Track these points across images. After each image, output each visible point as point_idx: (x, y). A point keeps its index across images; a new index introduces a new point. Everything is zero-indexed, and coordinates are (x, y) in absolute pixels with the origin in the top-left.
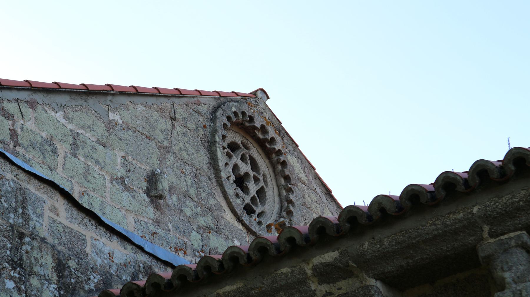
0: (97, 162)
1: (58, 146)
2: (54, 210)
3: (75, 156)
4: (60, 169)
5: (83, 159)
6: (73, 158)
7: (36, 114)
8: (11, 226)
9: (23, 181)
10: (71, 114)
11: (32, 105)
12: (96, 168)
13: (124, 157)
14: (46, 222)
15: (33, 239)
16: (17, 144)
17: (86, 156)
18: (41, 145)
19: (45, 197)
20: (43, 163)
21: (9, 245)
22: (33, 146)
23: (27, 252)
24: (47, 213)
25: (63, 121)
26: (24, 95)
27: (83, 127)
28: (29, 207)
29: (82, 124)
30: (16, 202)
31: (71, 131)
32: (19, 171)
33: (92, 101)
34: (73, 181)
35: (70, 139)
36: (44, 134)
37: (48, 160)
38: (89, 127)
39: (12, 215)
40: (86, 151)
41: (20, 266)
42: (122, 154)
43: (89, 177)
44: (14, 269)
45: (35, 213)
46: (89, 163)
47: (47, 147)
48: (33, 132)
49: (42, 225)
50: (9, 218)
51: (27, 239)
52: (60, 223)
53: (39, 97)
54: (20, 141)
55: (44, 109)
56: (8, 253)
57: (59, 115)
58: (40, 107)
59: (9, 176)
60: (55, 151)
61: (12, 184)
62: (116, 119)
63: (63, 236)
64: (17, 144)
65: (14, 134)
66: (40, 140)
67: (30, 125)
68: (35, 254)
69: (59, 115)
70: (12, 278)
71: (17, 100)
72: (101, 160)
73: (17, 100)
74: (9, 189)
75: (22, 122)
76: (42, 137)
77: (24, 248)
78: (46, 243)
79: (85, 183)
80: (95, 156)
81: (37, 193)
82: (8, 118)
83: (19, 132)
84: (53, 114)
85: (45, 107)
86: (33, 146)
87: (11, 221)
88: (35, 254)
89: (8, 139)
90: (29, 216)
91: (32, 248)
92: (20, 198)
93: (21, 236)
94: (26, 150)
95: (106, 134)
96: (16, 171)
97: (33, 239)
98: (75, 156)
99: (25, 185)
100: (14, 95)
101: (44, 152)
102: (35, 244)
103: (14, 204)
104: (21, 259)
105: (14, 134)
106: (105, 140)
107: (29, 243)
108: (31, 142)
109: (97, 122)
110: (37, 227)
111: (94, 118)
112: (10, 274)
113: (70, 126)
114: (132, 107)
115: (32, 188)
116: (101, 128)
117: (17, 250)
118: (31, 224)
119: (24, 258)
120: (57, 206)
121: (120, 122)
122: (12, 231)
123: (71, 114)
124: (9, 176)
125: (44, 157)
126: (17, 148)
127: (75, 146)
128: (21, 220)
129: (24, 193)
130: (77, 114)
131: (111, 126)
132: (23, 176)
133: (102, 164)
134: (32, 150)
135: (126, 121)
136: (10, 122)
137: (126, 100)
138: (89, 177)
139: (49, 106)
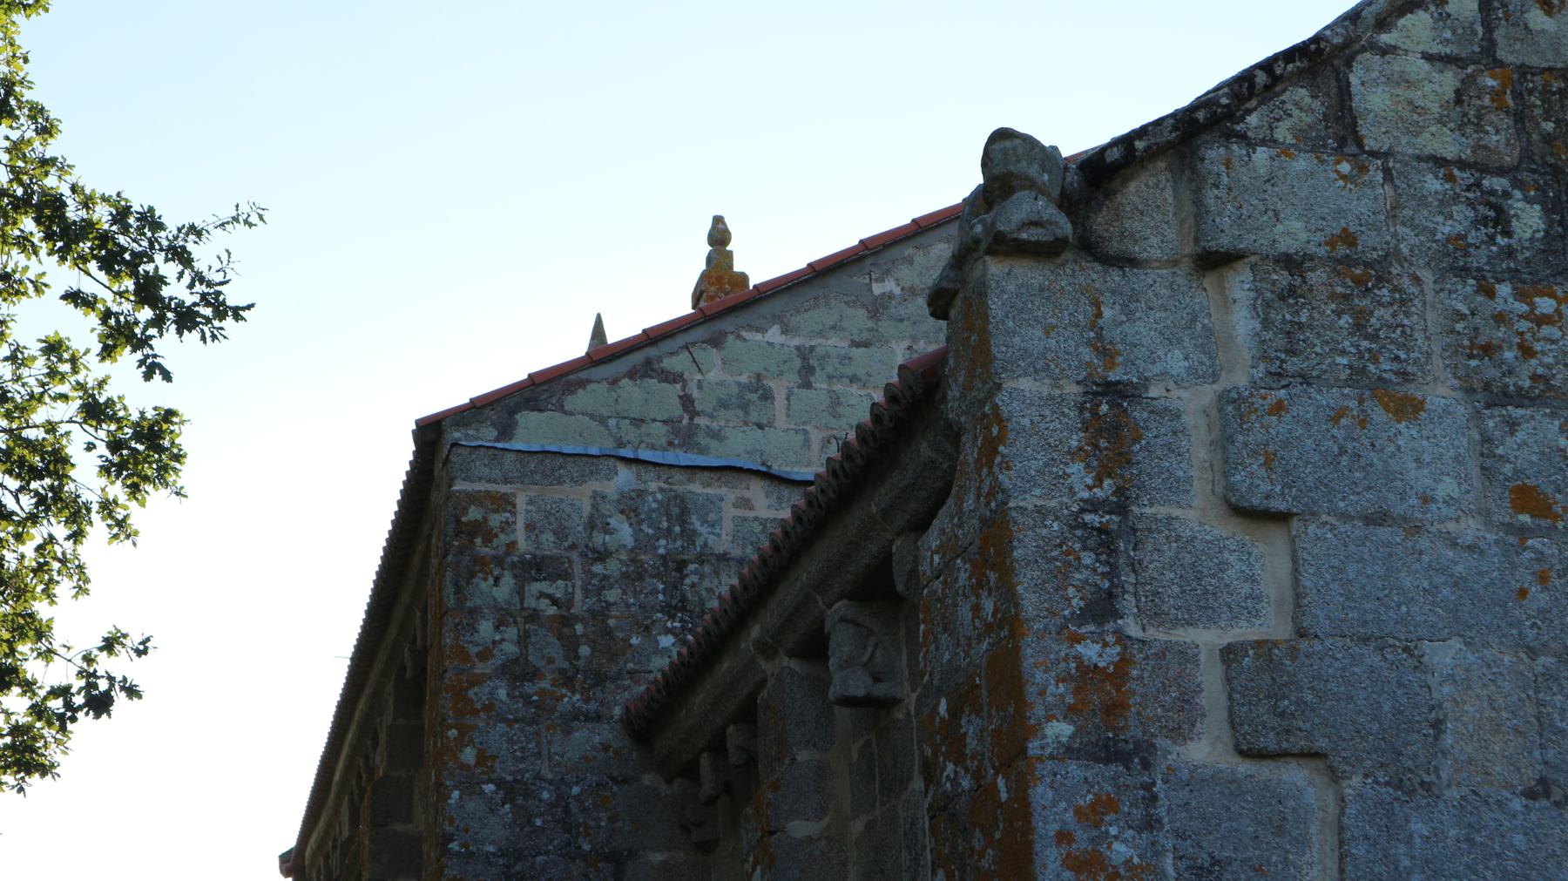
0: (853, 379)
1: (771, 384)
2: (745, 503)
3: (807, 385)
4: (781, 420)
5: (824, 386)
6: (804, 393)
7: (723, 352)
8: (663, 557)
9: (680, 483)
10: (795, 320)
11: (716, 342)
12: (854, 389)
13: (909, 348)
14: (728, 526)
15: (702, 563)
16: (694, 414)
17: (830, 377)
18: (740, 397)
19: (723, 491)
20: (746, 423)
21: (661, 587)
22: (724, 405)
23: (693, 585)
24: (729, 512)
25: (781, 339)
26: (700, 333)
27: (821, 334)
28: (694, 519)
29: (818, 328)
30: (669, 521)
31: (798, 348)
32: (673, 472)
33: (832, 281)
34: (808, 428)
35: (797, 363)
36: (744, 379)
37: (754, 416)
38: (833, 327)
39: (663, 542)
40: (829, 369)
41: (683, 609)
42: (906, 344)
43: (840, 410)
44: (672, 617)
45: (704, 522)
46: (838, 387)
47: (754, 397)
48: (721, 384)
49: (719, 535)
50: (656, 548)
51: (692, 567)
52: (756, 519)
53: (726, 324)
54: (699, 408)
55: (739, 337)
56: (661, 597)
57: (774, 334)
58: (731, 338)
59: (653, 486)
60: (767, 396)
61: (659, 496)
62: (887, 289)
63: (762, 538)
64: (694, 414)
65: (687, 401)
66: (735, 390)
67: (714, 375)
68: (707, 583)
69: (774, 334)
70: (668, 631)
71: (686, 347)
72: (861, 372)
73: (686, 347)
74: (654, 505)
75: (699, 377)
76: (739, 384)
77: (687, 581)
78: (728, 560)
79: (833, 422)
80: (848, 371)
81: (709, 491)
82: (675, 381)
83: (695, 393)
84: (759, 336)
85: (744, 334)
86: (724, 405)
87: (662, 551)
88: (707, 583)
89: (676, 409)
90: (694, 531)
91: (702, 577)
92: (675, 511)
93: (681, 566)
94: (711, 416)
95: (870, 324)
96: (665, 474)
97: (702, 563)
98: (807, 385)
99: (679, 489)
100: (681, 340)
101: (745, 407)
102: (707, 569)
103: (665, 524)
104: (683, 599)
105: (687, 401)
106: (866, 336)
107: (695, 572)
108: (719, 400)
109: (851, 312)
110: (710, 542)
111: (843, 306)
112: (665, 627)
113: (796, 342)
114: (919, 258)
115: (697, 488)
116: (858, 319)
117: (675, 588)
118: (699, 542)
119: (689, 595)
120: (747, 494)
121: (897, 291)
122: (665, 564)
123: (795, 320)
124: (653, 486)
125: (747, 413)
126: (697, 420)
127: (807, 371)
128: (679, 543)
129: (683, 500)
130: (806, 316)
131: (877, 308)
132: (678, 476)
133: (865, 378)
134: (722, 412)
135: (907, 284)
136: (678, 386)
137: (908, 250)
138: (840, 410)
139: (750, 328)
